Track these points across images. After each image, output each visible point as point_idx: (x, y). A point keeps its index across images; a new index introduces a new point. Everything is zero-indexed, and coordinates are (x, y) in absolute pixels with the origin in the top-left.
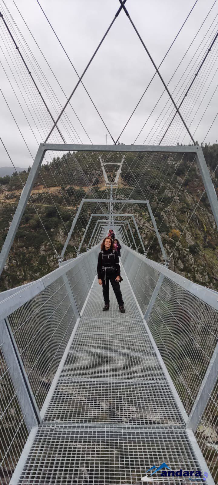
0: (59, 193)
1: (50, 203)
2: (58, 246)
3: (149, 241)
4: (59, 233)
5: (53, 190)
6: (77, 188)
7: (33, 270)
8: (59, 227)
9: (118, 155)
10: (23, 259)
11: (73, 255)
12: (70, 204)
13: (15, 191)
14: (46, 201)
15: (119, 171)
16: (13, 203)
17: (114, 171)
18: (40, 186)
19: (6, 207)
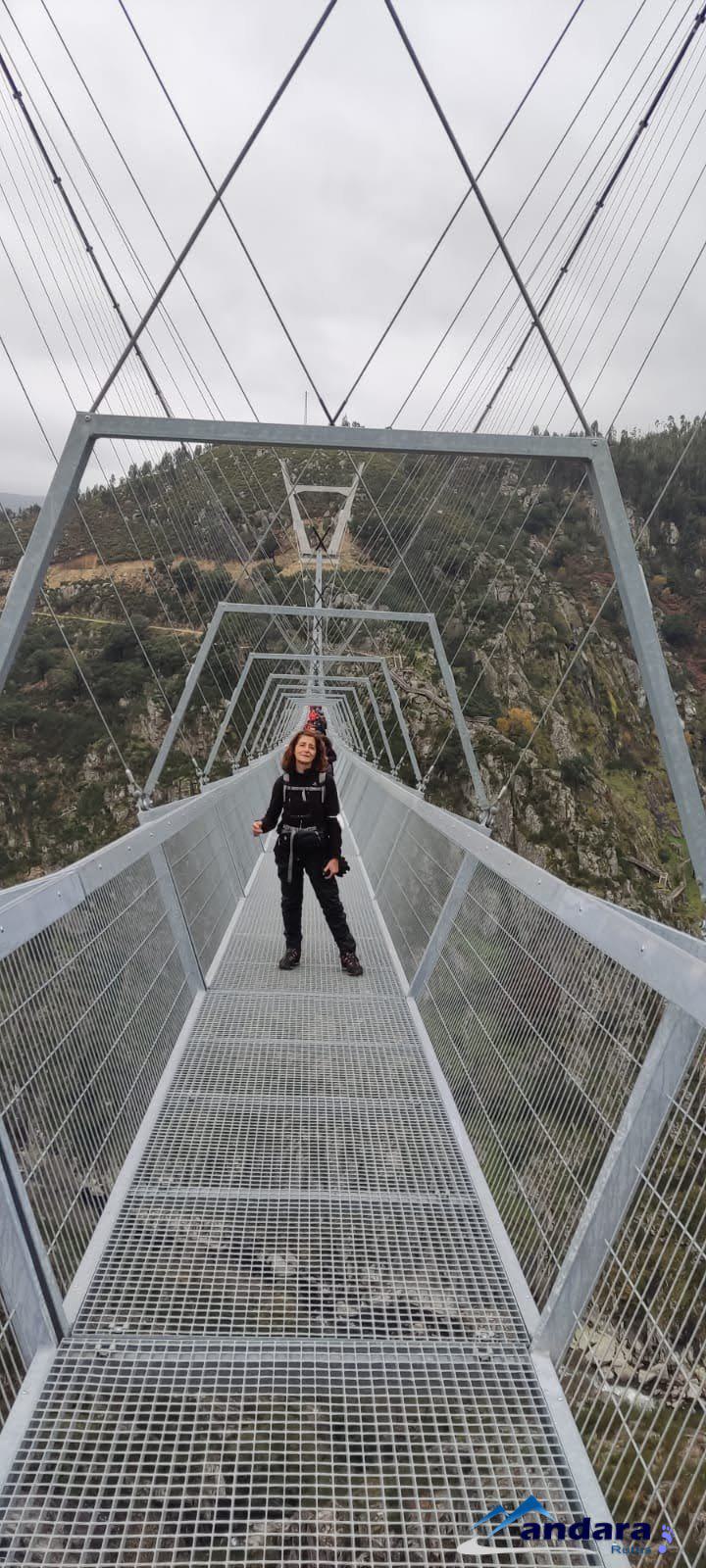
0: (148, 581)
1: (117, 613)
2: (142, 755)
3: (436, 746)
4: (146, 713)
5: (127, 572)
6: (206, 566)
7: (61, 832)
8: (145, 693)
9: (342, 463)
10: (27, 795)
11: (192, 784)
12: (181, 619)
14: (104, 607)
15: (344, 516)
17: (327, 514)
18: (87, 559)
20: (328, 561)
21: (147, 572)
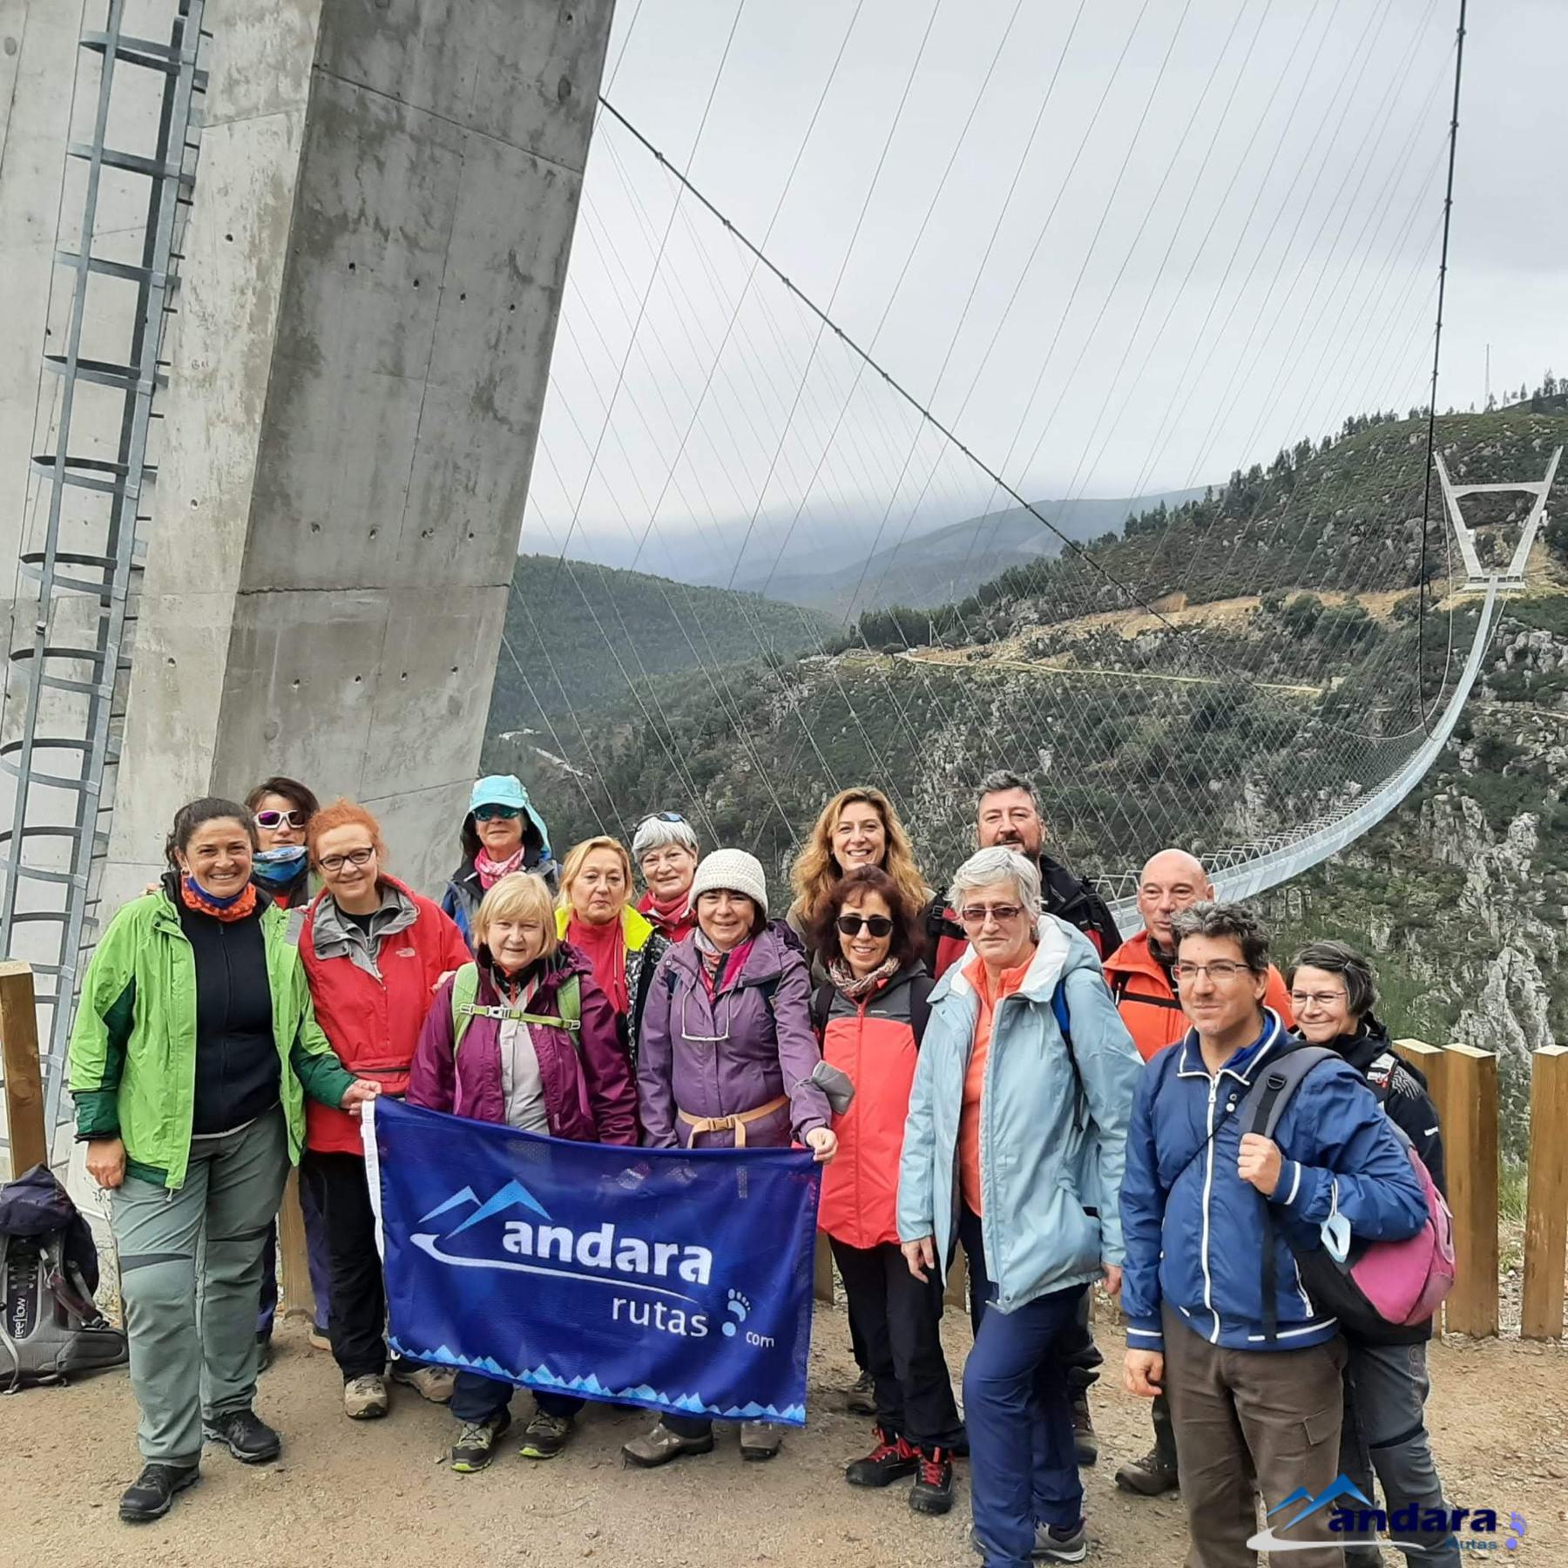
0: (1250, 623)
1: (1207, 669)
4: (1245, 802)
5: (1227, 614)
6: (1332, 601)
9: (1537, 443)
11: (1303, 895)
13: (1067, 623)
15: (1539, 515)
16: (1057, 674)
17: (1512, 517)
18: (1171, 599)
19: (1030, 689)
20: (1503, 586)
21: (1251, 612)
